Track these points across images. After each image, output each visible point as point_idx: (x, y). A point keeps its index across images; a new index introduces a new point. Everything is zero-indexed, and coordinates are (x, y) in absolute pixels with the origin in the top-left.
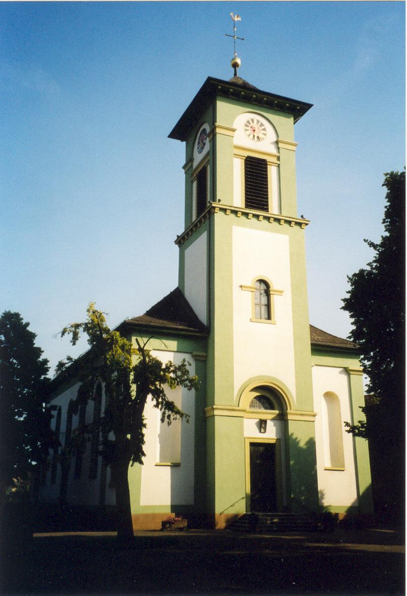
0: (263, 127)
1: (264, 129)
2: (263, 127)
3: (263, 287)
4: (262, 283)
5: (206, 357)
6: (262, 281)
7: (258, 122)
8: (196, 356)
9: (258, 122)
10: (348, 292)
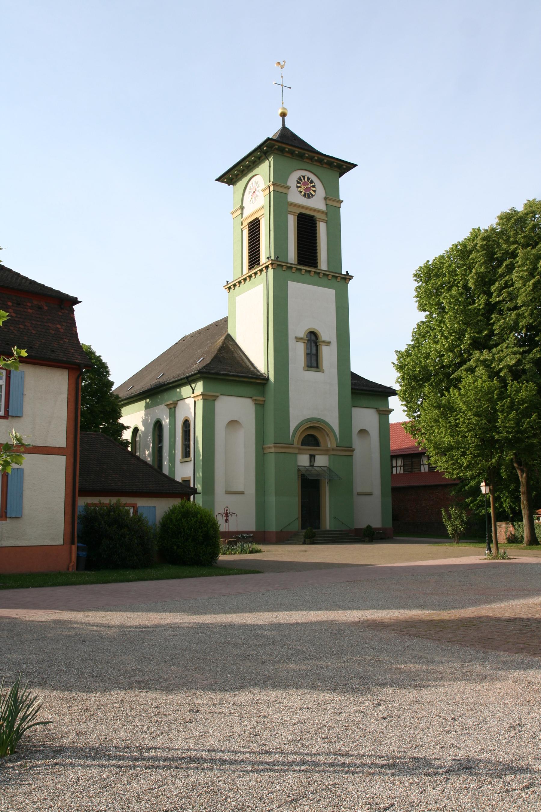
0: (313, 184)
1: (314, 186)
2: (313, 184)
3: (313, 338)
4: (312, 334)
5: (265, 401)
6: (286, 148)
7: (308, 179)
8: (256, 400)
9: (308, 179)
10: (347, 272)
